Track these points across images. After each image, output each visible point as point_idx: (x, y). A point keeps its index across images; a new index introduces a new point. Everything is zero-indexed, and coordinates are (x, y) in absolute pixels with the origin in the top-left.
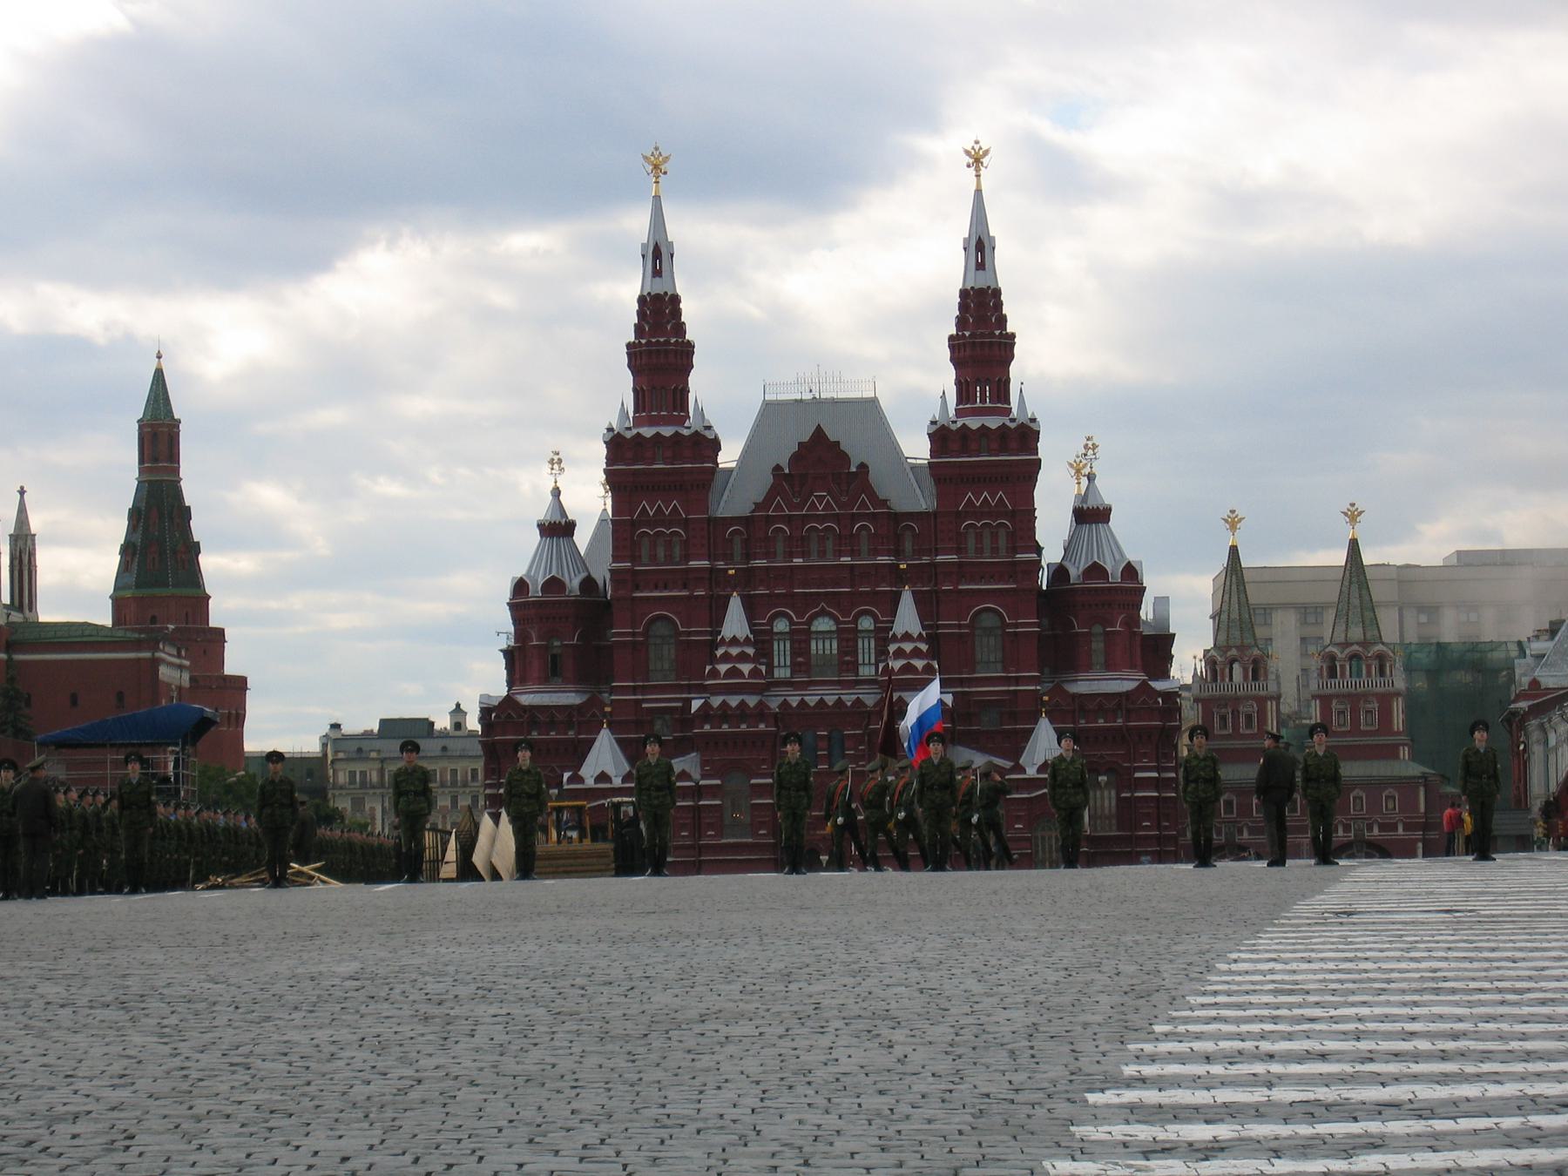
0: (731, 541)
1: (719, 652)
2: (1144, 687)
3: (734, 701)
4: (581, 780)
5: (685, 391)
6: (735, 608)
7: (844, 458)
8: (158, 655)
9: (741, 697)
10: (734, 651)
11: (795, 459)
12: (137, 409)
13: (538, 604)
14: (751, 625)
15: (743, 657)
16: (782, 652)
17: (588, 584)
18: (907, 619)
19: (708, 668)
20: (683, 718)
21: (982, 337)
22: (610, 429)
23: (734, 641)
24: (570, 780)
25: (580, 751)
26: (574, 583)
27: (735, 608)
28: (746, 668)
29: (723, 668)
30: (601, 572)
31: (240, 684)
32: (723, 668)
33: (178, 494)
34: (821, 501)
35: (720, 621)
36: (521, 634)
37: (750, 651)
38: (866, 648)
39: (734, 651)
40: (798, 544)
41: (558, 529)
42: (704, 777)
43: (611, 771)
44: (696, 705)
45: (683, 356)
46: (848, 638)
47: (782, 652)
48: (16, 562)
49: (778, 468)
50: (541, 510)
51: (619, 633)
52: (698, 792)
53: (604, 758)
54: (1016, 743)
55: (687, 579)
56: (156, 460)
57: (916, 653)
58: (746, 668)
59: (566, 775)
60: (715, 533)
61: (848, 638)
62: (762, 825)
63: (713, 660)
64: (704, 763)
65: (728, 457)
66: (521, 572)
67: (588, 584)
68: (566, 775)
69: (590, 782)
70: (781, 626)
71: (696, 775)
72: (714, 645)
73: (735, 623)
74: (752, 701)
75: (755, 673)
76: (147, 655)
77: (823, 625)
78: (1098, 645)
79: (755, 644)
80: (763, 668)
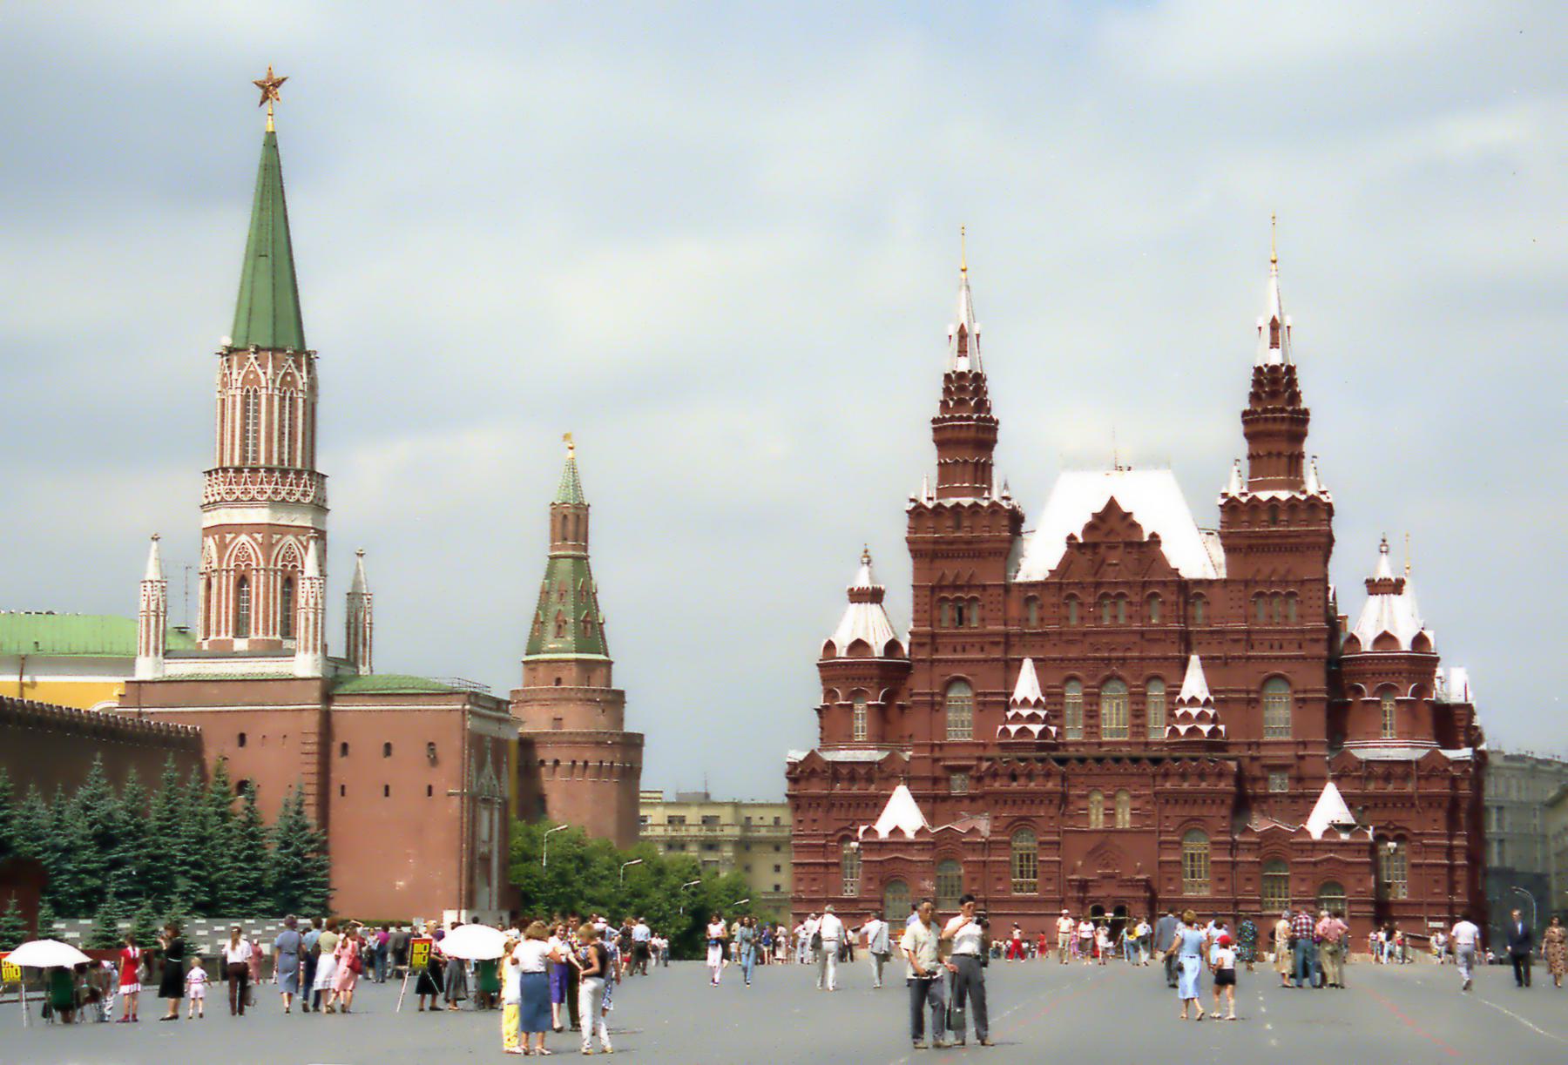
2: (1434, 754)
7: (1136, 527)
11: (1090, 528)
15: (1033, 718)
17: (892, 646)
18: (1195, 683)
21: (1276, 414)
25: (878, 804)
36: (830, 694)
39: (1025, 712)
49: (1071, 538)
53: (902, 813)
57: (1202, 717)
58: (1036, 729)
73: (1027, 685)
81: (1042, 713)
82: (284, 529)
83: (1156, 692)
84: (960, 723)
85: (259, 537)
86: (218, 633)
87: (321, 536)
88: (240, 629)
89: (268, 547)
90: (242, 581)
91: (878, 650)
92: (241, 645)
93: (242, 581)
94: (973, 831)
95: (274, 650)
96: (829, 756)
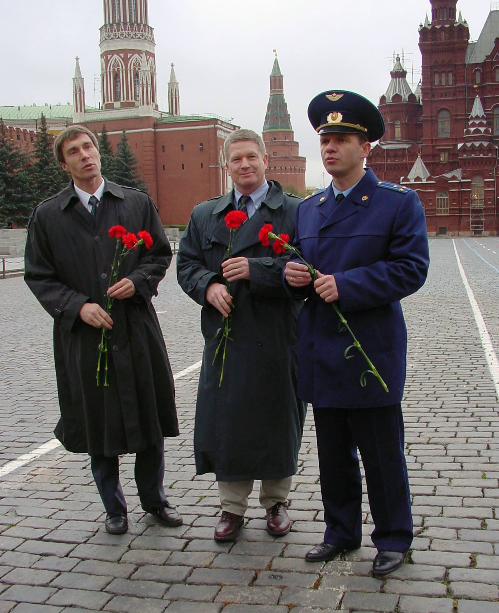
0: (475, 74)
1: (470, 123)
3: (477, 144)
4: (408, 180)
5: (454, 10)
8: (216, 126)
9: (480, 142)
10: (477, 122)
12: (269, 72)
13: (390, 106)
14: (485, 111)
15: (481, 125)
19: (465, 130)
20: (454, 153)
22: (421, 26)
23: (477, 117)
24: (403, 180)
25: (407, 169)
26: (405, 97)
28: (482, 129)
29: (472, 129)
30: (419, 95)
31: (303, 160)
32: (472, 129)
33: (283, 99)
35: (470, 110)
37: (485, 122)
39: (477, 122)
41: (399, 74)
42: (463, 178)
43: (422, 176)
44: (460, 146)
48: (170, 94)
50: (392, 67)
52: (461, 184)
53: (419, 171)
56: (275, 88)
58: (482, 129)
59: (402, 178)
62: (490, 200)
63: (469, 126)
64: (463, 172)
65: (474, 36)
66: (383, 92)
67: (412, 97)
68: (402, 178)
69: (412, 182)
71: (460, 179)
72: (468, 120)
73: (477, 109)
74: (485, 144)
75: (486, 131)
76: (212, 126)
79: (486, 119)
80: (490, 129)
81: (485, 122)
82: (134, 52)
84: (445, 129)
85: (122, 55)
86: (108, 101)
87: (153, 55)
88: (116, 99)
89: (126, 60)
90: (116, 76)
92: (117, 105)
93: (116, 76)
94: (454, 178)
95: (131, 105)
96: (384, 147)
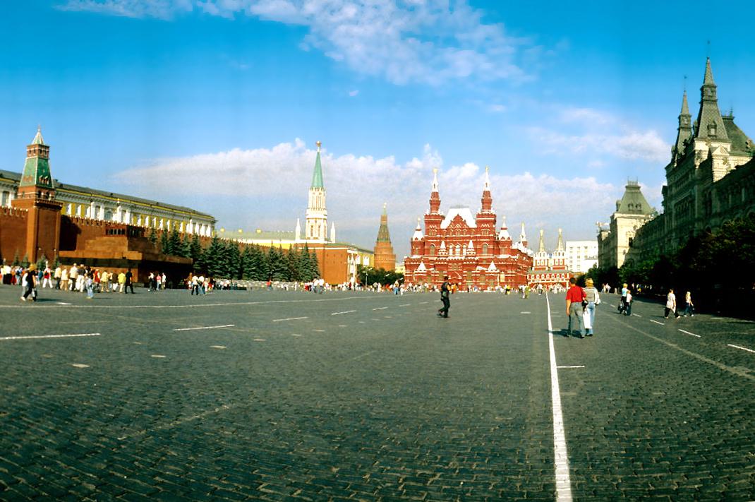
6: (443, 243)
16: (451, 251)
18: (471, 245)
27: (443, 243)
34: (458, 226)
38: (464, 250)
40: (454, 233)
45: (438, 203)
46: (462, 249)
47: (451, 251)
51: (426, 247)
52: (435, 273)
53: (422, 267)
54: (488, 266)
55: (436, 238)
60: (440, 231)
61: (462, 249)
70: (451, 247)
73: (443, 245)
77: (457, 246)
78: (503, 250)
83: (465, 246)
91: (420, 239)
